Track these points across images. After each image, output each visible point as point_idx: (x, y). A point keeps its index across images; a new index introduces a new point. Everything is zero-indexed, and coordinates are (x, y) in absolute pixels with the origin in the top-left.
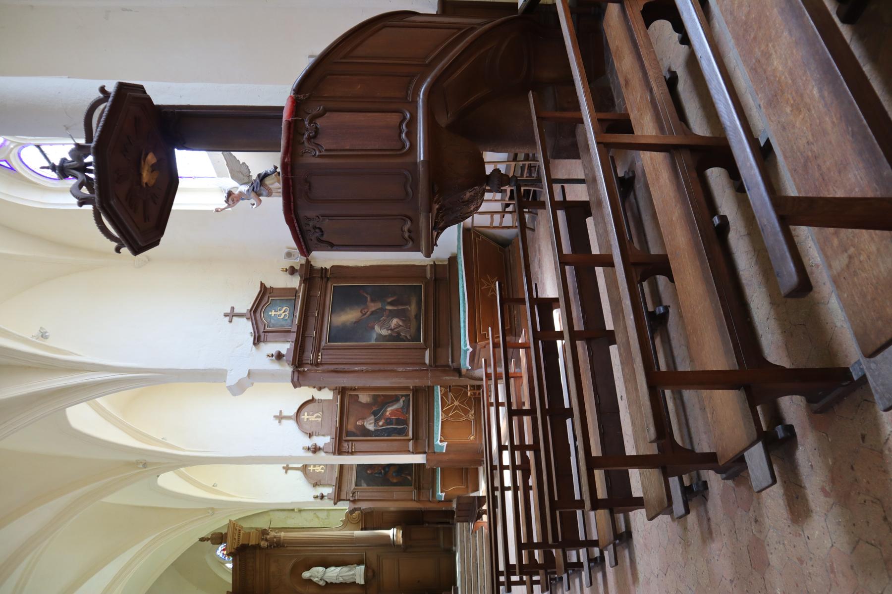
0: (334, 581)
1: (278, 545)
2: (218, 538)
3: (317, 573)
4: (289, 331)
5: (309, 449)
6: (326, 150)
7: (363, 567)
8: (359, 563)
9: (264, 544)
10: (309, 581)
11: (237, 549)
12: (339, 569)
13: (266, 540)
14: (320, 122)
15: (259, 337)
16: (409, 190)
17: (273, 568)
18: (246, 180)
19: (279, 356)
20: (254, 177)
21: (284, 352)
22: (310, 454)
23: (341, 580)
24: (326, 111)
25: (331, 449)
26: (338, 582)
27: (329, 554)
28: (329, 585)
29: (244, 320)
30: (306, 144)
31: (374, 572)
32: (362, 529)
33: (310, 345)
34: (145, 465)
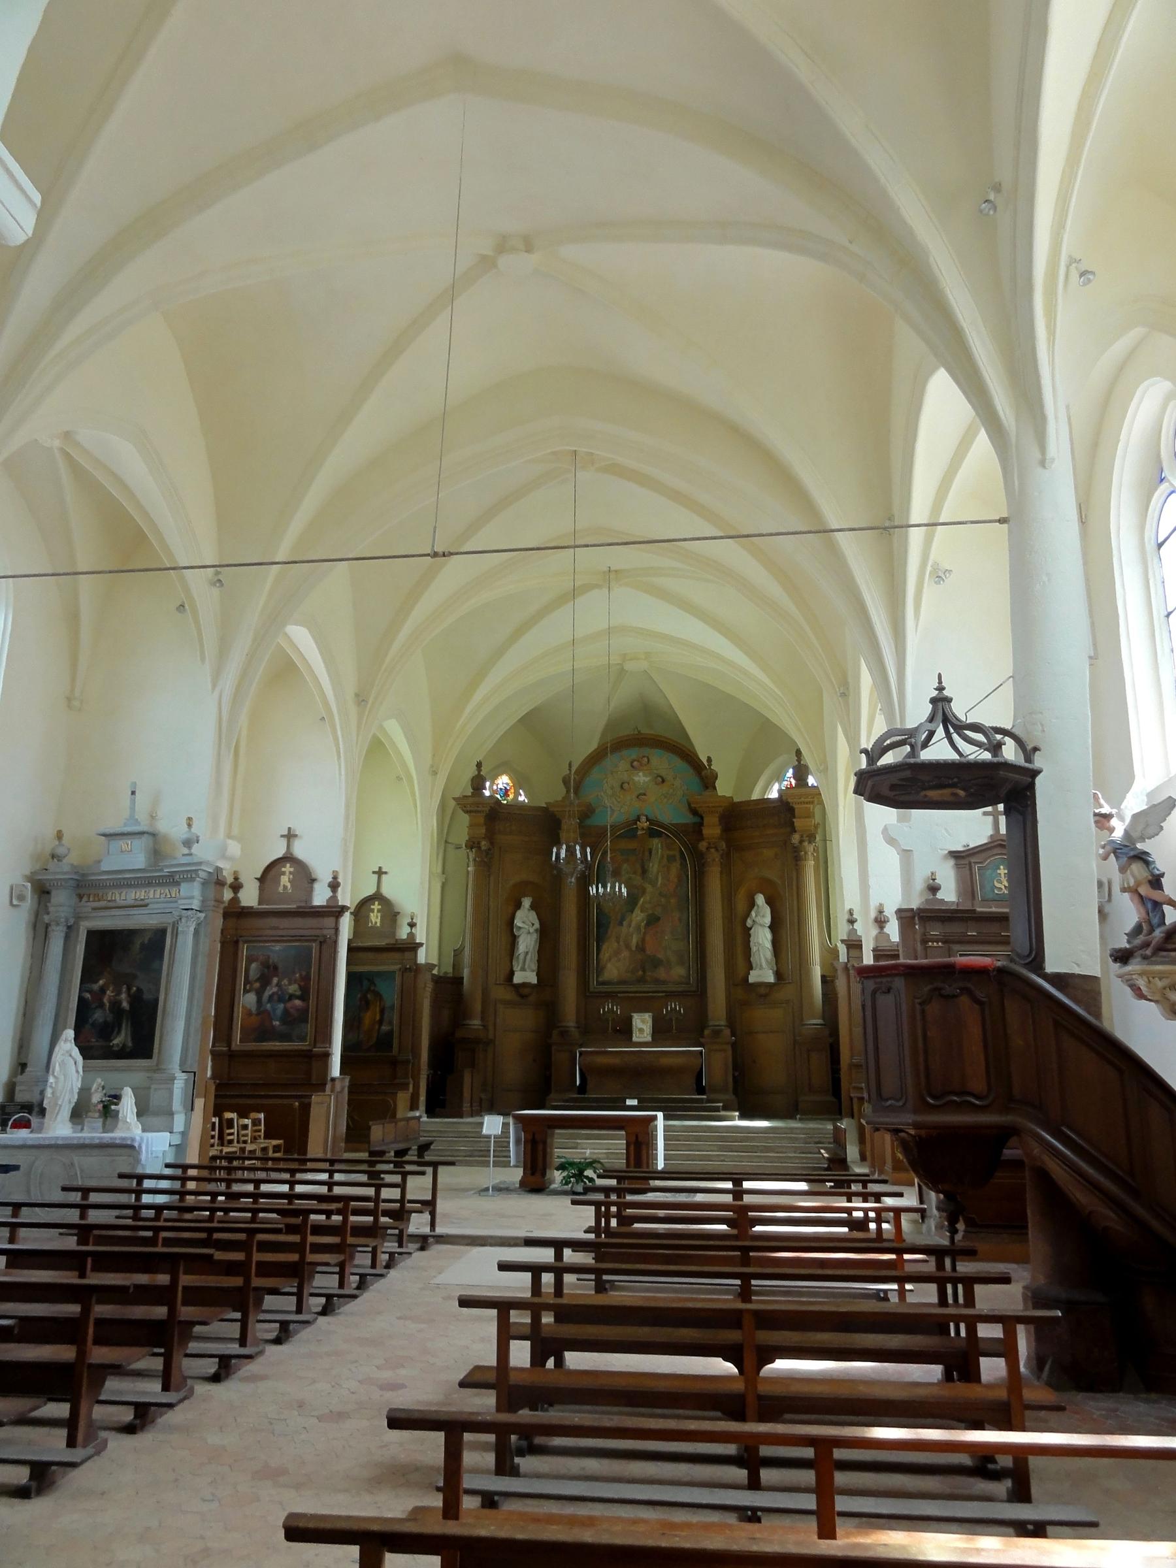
0: (752, 939)
1: (797, 858)
3: (762, 915)
4: (974, 895)
5: (881, 912)
6: (923, 1012)
7: (771, 979)
8: (778, 975)
9: (796, 839)
10: (752, 904)
11: (788, 803)
12: (768, 945)
13: (801, 842)
14: (964, 1000)
15: (963, 857)
16: (889, 1102)
17: (768, 853)
18: (1135, 835)
19: (934, 889)
20: (1139, 846)
21: (939, 895)
22: (873, 914)
23: (754, 949)
25: (884, 945)
26: (752, 944)
28: (747, 932)
29: (990, 832)
30: (929, 987)
31: (765, 996)
32: (823, 977)
33: (955, 929)
34: (844, 695)
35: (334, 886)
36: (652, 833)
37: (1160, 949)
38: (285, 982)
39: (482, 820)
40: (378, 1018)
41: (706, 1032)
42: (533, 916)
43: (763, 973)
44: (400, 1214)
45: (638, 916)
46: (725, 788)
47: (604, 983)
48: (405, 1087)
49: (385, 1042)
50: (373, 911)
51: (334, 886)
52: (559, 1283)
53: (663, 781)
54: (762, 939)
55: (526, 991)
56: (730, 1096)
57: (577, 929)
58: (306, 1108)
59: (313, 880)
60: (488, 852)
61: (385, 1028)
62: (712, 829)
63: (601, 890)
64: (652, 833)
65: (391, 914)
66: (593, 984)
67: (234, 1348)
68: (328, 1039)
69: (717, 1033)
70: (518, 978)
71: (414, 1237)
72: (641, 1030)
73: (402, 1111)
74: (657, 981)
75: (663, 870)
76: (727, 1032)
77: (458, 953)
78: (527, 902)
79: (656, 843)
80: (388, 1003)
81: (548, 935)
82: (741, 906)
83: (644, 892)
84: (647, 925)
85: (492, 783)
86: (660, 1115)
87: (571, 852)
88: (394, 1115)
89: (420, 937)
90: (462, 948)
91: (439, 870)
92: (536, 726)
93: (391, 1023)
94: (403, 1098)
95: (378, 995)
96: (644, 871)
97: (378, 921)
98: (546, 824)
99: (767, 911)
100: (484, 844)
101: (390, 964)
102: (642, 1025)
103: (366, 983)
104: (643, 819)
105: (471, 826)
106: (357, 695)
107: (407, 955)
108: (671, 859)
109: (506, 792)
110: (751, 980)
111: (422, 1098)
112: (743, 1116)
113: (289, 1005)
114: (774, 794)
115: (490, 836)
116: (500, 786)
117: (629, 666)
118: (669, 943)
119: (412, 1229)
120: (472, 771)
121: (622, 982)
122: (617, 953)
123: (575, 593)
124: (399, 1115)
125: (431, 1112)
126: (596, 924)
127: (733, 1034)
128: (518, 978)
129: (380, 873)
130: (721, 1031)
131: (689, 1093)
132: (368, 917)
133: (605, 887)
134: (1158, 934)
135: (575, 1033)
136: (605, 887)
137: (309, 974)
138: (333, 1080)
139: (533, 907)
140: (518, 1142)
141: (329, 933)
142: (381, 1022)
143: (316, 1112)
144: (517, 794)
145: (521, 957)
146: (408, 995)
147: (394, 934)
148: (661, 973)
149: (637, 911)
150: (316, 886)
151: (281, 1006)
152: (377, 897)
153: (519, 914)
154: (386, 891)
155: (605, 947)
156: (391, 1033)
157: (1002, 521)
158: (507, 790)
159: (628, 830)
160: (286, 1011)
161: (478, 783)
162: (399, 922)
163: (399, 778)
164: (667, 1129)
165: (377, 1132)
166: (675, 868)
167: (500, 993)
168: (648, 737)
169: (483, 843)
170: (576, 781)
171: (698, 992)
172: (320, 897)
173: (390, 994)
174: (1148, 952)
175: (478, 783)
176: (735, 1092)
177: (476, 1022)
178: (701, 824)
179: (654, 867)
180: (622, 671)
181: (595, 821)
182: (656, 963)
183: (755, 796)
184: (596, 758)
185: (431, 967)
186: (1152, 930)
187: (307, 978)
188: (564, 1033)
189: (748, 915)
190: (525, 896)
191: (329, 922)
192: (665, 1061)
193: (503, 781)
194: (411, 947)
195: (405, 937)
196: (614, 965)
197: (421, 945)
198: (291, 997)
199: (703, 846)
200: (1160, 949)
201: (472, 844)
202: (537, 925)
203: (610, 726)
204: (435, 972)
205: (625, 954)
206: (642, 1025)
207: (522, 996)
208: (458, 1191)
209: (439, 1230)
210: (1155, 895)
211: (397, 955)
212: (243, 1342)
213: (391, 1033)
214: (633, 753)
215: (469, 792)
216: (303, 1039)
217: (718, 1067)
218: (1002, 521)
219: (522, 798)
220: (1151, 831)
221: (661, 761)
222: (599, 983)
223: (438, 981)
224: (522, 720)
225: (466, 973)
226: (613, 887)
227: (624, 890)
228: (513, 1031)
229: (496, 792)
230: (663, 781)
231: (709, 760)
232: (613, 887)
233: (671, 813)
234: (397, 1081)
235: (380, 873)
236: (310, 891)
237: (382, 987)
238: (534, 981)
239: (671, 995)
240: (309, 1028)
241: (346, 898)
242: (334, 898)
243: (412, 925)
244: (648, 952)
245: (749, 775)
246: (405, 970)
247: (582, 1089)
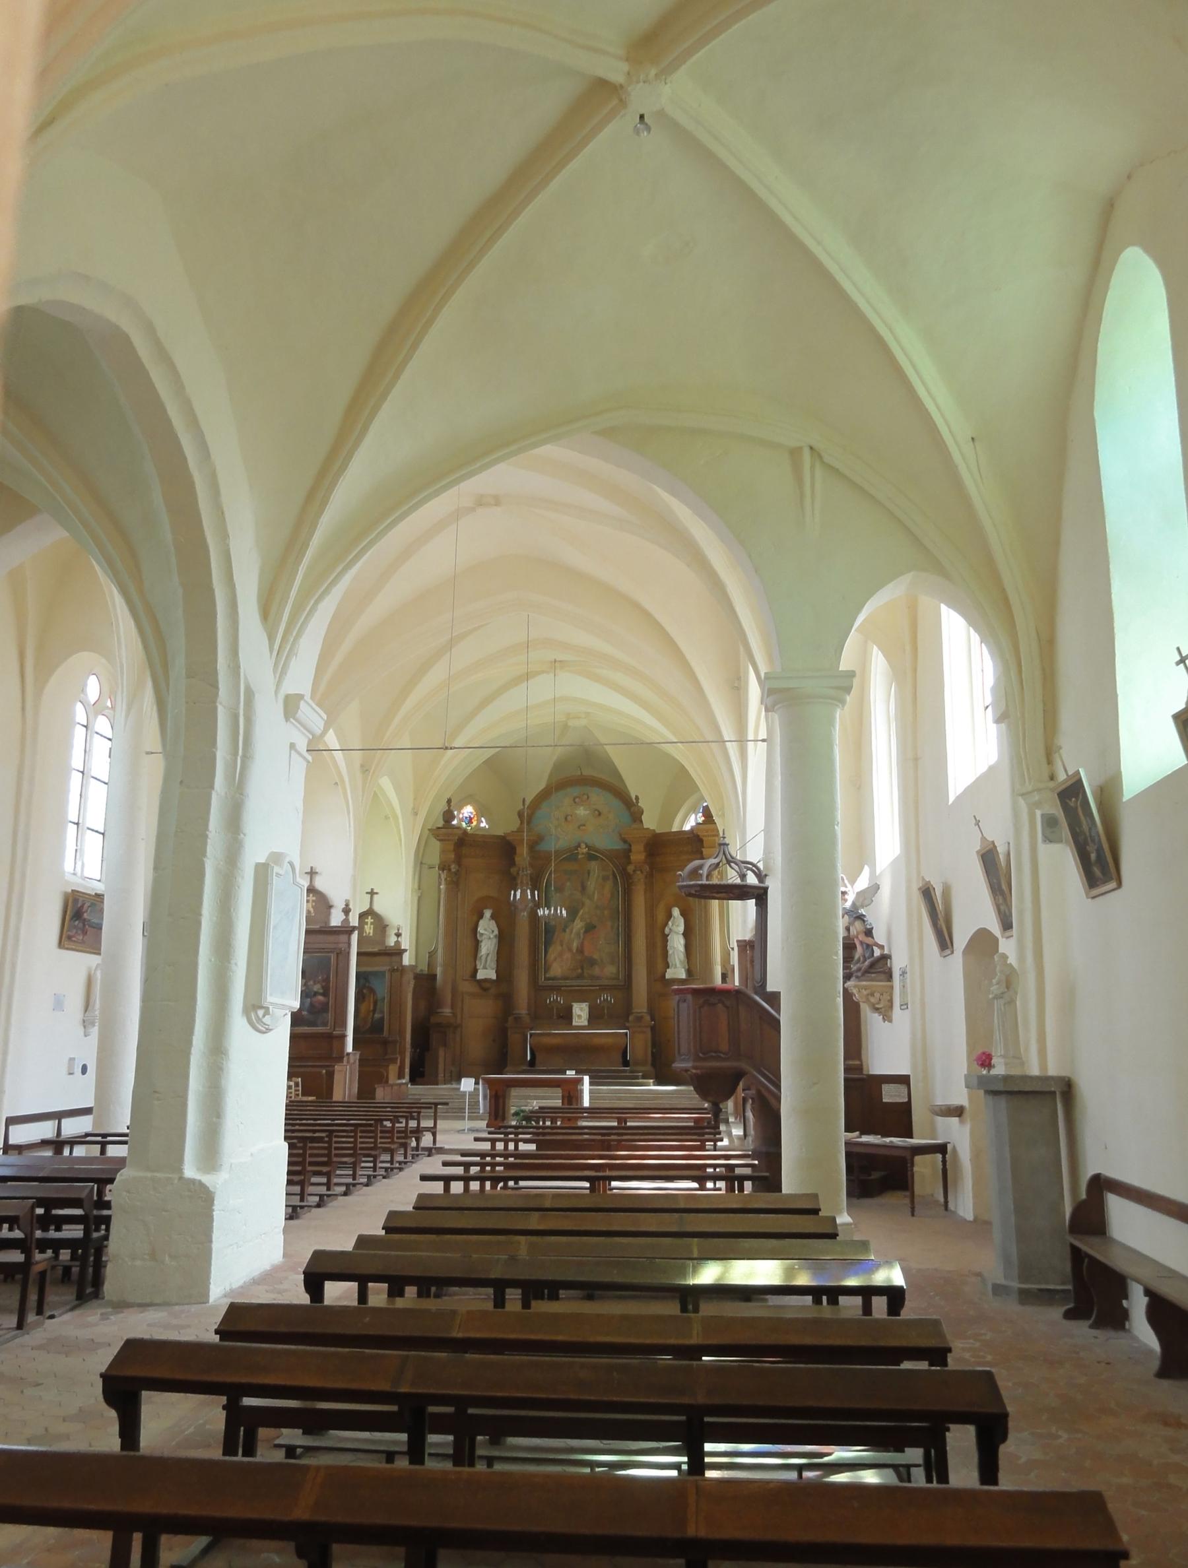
2: (707, 813)
7: (683, 976)
8: (689, 972)
12: (682, 949)
14: (720, 1005)
23: (670, 952)
24: (727, 1007)
27: (695, 936)
28: (665, 938)
35: (347, 911)
36: (591, 857)
37: (867, 972)
38: (311, 983)
39: (452, 848)
41: (631, 1018)
42: (493, 925)
43: (677, 971)
44: (418, 1132)
45: (578, 925)
46: (651, 822)
47: (549, 979)
48: (394, 1061)
51: (347, 911)
52: (516, 1147)
53: (600, 814)
54: (677, 943)
55: (487, 985)
56: (648, 1068)
57: (526, 941)
58: (331, 1075)
59: (331, 907)
60: (456, 874)
61: (377, 1016)
62: (638, 855)
63: (547, 912)
64: (591, 857)
65: (381, 926)
66: (542, 981)
67: (350, 1180)
68: (344, 1024)
69: (639, 1019)
70: (481, 975)
71: (424, 1149)
72: (579, 1016)
73: (393, 1079)
74: (593, 977)
75: (598, 887)
76: (648, 1018)
77: (432, 955)
78: (488, 913)
79: (594, 865)
80: (379, 996)
81: (505, 940)
82: (661, 917)
83: (583, 904)
84: (586, 932)
85: (459, 812)
86: (586, 1079)
87: (523, 893)
88: (387, 1082)
89: (406, 943)
91: (416, 886)
92: (497, 767)
93: (382, 1012)
94: (393, 1070)
95: (372, 991)
96: (584, 888)
98: (504, 848)
99: (681, 921)
100: (454, 868)
101: (381, 966)
102: (581, 1013)
104: (583, 846)
105: (443, 852)
106: (362, 766)
107: (395, 959)
108: (605, 878)
109: (470, 820)
110: (668, 976)
111: (407, 1070)
112: (659, 1082)
113: (314, 999)
114: (687, 827)
115: (459, 860)
116: (466, 815)
117: (571, 723)
118: (603, 947)
119: (422, 1145)
120: (442, 806)
121: (566, 978)
122: (561, 954)
123: (527, 676)
124: (391, 1082)
125: (413, 1080)
126: (543, 934)
127: (653, 1019)
128: (481, 975)
130: (642, 1017)
131: (614, 1065)
133: (549, 908)
134: (867, 963)
135: (527, 1020)
136: (549, 908)
137: (328, 977)
138: (348, 1054)
139: (493, 917)
140: (485, 1097)
141: (343, 946)
142: (374, 1011)
143: (337, 1078)
144: (479, 822)
145: (483, 959)
146: (396, 991)
147: (384, 942)
148: (596, 971)
149: (577, 921)
150: (333, 911)
151: (309, 1000)
152: (370, 912)
153: (481, 922)
155: (551, 950)
157: (763, 741)
158: (471, 819)
159: (570, 855)
160: (311, 1003)
161: (448, 816)
163: (387, 818)
164: (591, 1092)
165: (381, 1094)
166: (609, 885)
167: (466, 987)
168: (586, 775)
170: (528, 814)
171: (626, 986)
172: (336, 919)
173: (382, 989)
174: (859, 974)
175: (448, 816)
176: (654, 1065)
177: (447, 1011)
178: (630, 851)
179: (591, 885)
180: (565, 727)
181: (545, 846)
182: (592, 962)
183: (674, 829)
184: (544, 795)
186: (865, 960)
187: (327, 980)
188: (518, 1019)
189: (666, 924)
190: (486, 908)
191: (343, 938)
192: (597, 1041)
193: (468, 810)
194: (398, 952)
195: (392, 944)
196: (559, 964)
197: (405, 950)
198: (316, 994)
199: (630, 868)
200: (867, 972)
201: (443, 867)
202: (496, 932)
203: (558, 766)
205: (567, 955)
206: (581, 1013)
207: (485, 990)
208: (446, 1131)
209: (438, 1145)
210: (868, 940)
211: (386, 959)
212: (354, 1177)
213: (382, 1019)
214: (575, 791)
215: (441, 823)
216: (325, 1024)
217: (639, 1045)
218: (763, 741)
219: (483, 825)
220: (866, 902)
221: (598, 798)
222: (546, 979)
223: (418, 977)
224: (486, 762)
225: (439, 971)
226: (556, 910)
227: (564, 912)
228: (475, 1020)
229: (462, 820)
230: (600, 814)
231: (637, 798)
232: (556, 910)
233: (606, 841)
235: (372, 893)
236: (328, 916)
238: (494, 977)
239: (604, 988)
240: (330, 1016)
241: (354, 921)
242: (346, 920)
243: (398, 935)
244: (586, 954)
245: (669, 812)
246: (393, 971)
247: (532, 1063)
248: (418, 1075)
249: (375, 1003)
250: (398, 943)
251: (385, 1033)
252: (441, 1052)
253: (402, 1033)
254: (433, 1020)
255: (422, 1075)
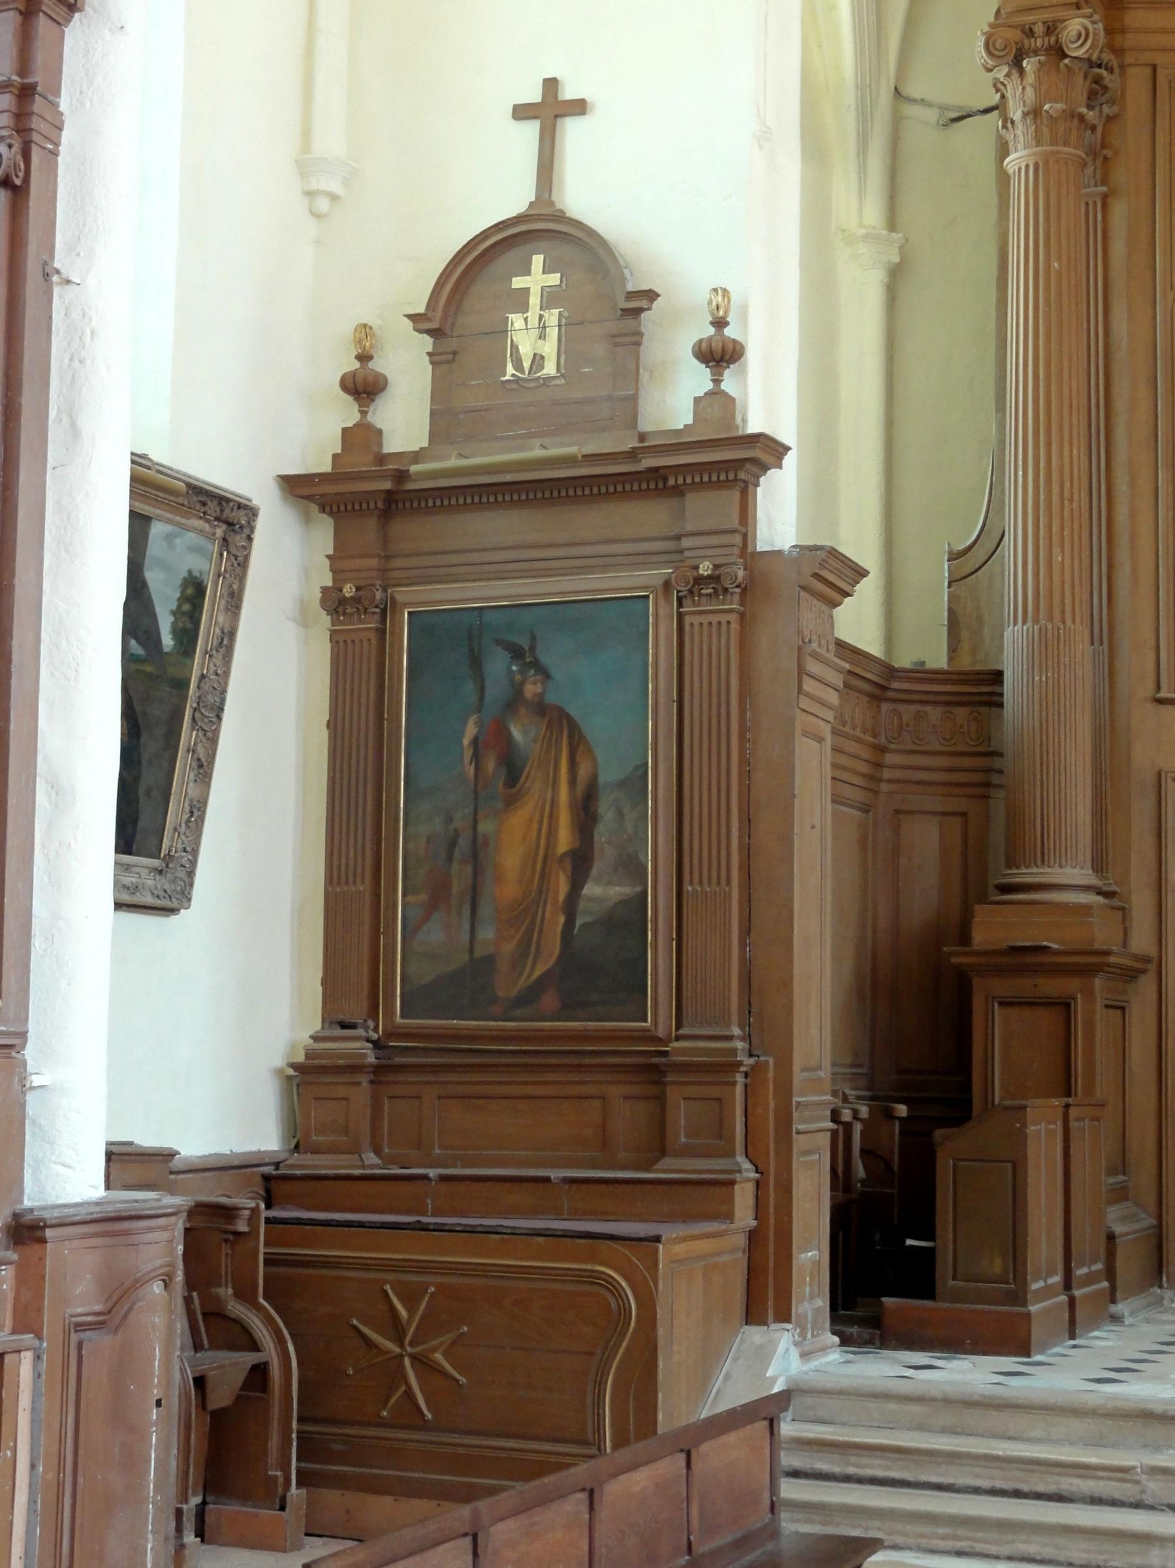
40: (565, 840)
48: (705, 1197)
49: (603, 967)
50: (520, 300)
61: (602, 891)
65: (615, 306)
77: (968, 567)
89: (768, 400)
90: (990, 541)
91: (874, 214)
93: (632, 868)
94: (693, 1261)
95: (563, 726)
97: (549, 348)
101: (616, 560)
103: (498, 665)
107: (705, 509)
111: (811, 1256)
129: (551, 110)
132: (501, 331)
142: (581, 862)
146: (718, 737)
152: (540, 229)
154: (580, 198)
156: (629, 920)
162: (652, 351)
169: (1075, 25)
173: (624, 718)
177: (1070, 874)
185: (830, 575)
194: (732, 461)
204: (859, 621)
211: (648, 517)
213: (629, 920)
223: (878, 684)
234: (668, 1169)
235: (551, 110)
237: (578, 678)
243: (720, 355)
248: (887, 1271)
249: (586, 812)
250: (717, 403)
251: (658, 1015)
252: (1042, 1131)
253: (762, 1002)
254: (993, 929)
255: (919, 1278)
